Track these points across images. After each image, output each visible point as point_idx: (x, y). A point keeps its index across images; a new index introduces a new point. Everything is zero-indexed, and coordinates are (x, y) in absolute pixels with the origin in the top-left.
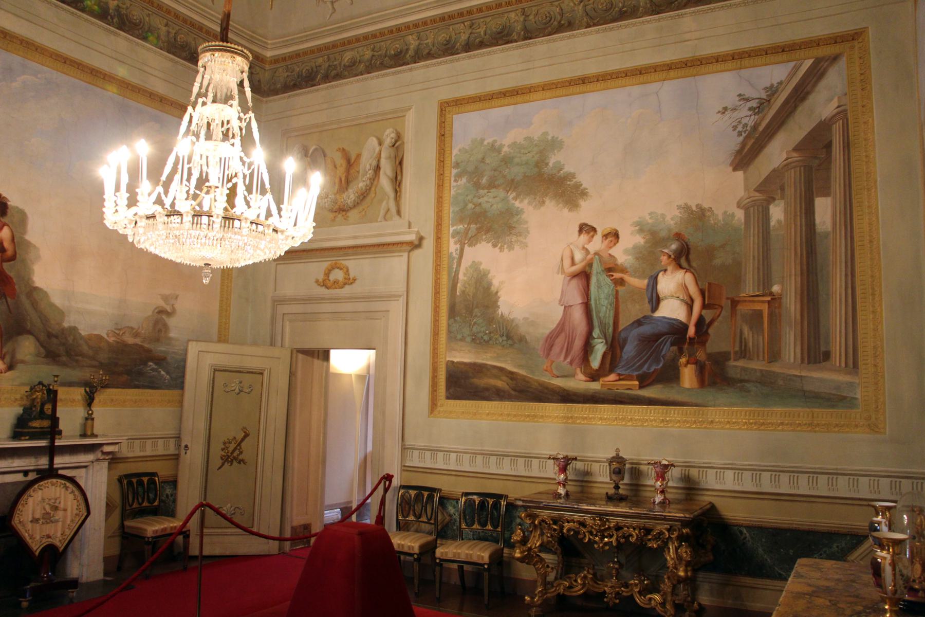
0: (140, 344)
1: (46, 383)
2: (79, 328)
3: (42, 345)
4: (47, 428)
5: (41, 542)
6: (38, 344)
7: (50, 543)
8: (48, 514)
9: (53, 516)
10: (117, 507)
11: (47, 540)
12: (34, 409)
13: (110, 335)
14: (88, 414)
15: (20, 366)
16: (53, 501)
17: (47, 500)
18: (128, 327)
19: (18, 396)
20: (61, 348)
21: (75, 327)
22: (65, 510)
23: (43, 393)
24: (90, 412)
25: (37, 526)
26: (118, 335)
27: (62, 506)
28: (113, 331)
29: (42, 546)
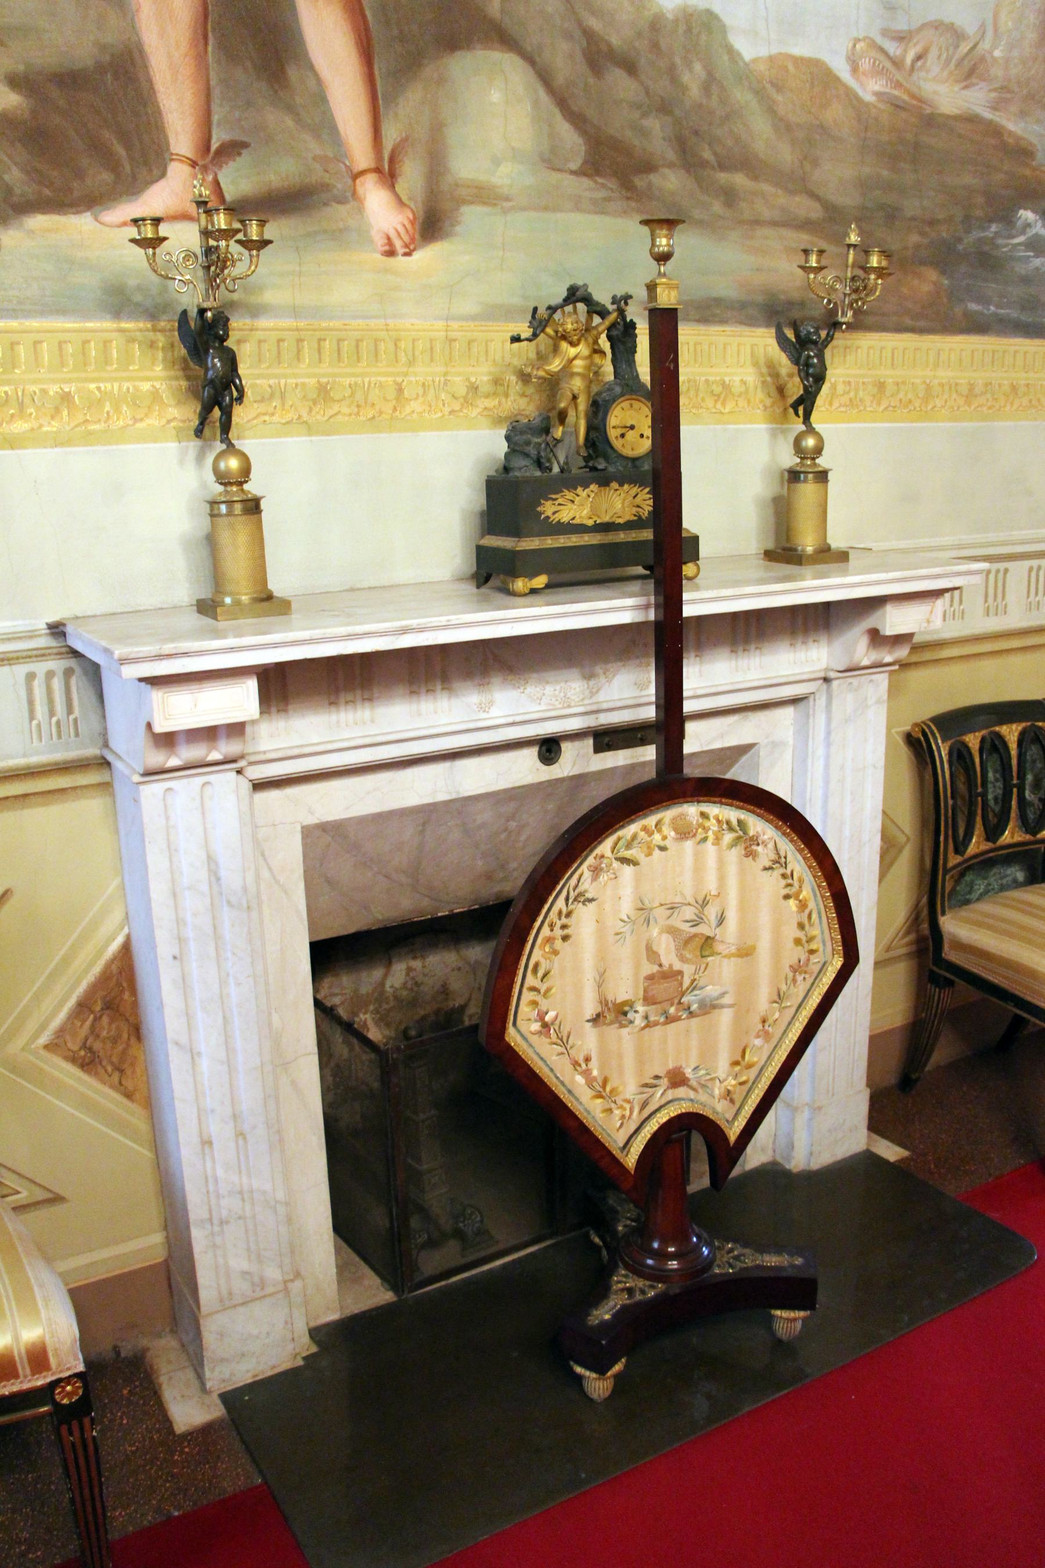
0: (988, 115)
1: (602, 296)
2: (727, 20)
3: (562, 102)
4: (629, 526)
5: (644, 1105)
6: (542, 93)
7: (684, 1108)
8: (672, 975)
9: (694, 986)
10: (900, 851)
11: (670, 1094)
12: (558, 432)
13: (865, 64)
14: (798, 446)
15: (471, 216)
16: (689, 913)
17: (660, 913)
18: (938, 26)
19: (482, 375)
20: (654, 124)
21: (709, 13)
22: (746, 952)
23: (599, 351)
24: (810, 442)
25: (625, 1038)
26: (898, 63)
27: (730, 934)
28: (873, 45)
29: (653, 1126)
